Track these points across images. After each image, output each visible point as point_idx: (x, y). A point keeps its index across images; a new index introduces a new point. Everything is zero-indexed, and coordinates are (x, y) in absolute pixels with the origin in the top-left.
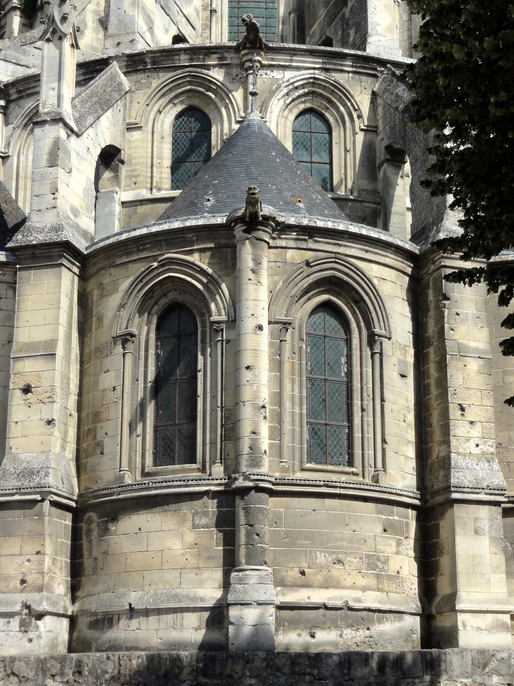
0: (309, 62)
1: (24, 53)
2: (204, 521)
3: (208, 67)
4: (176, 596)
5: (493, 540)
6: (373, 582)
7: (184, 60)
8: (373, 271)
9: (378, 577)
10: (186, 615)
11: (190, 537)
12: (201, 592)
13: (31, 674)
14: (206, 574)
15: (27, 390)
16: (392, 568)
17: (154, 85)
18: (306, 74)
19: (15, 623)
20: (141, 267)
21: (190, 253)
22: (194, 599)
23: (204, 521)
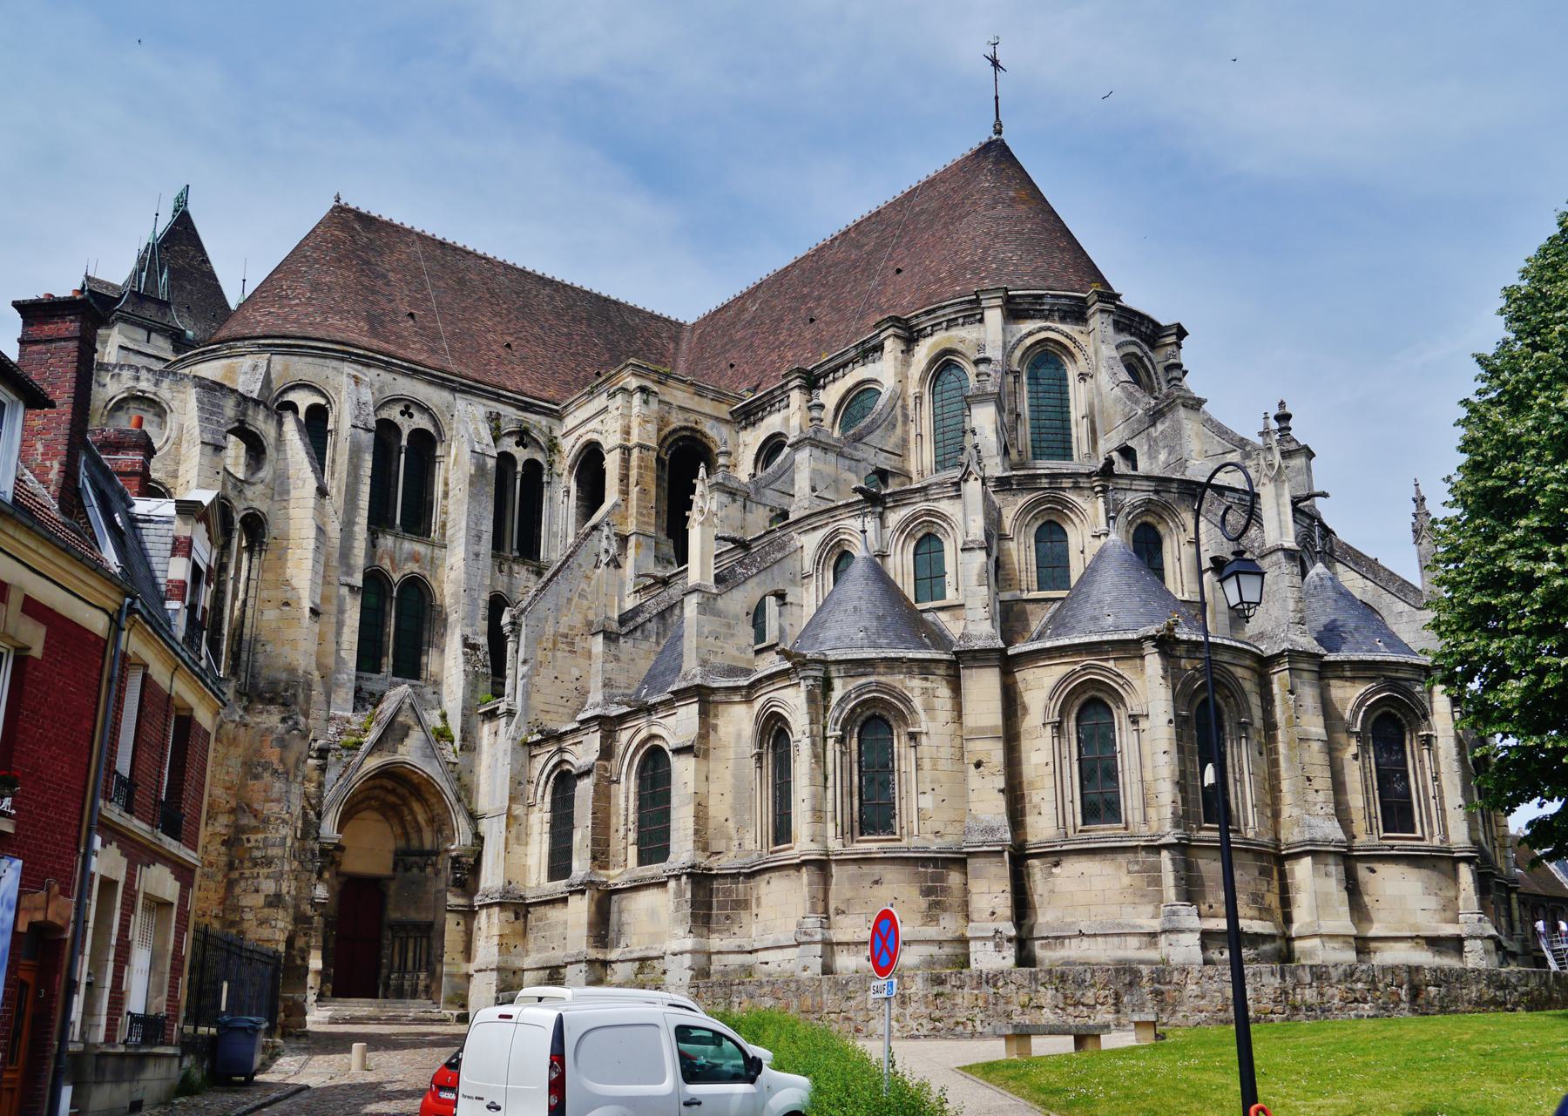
0: (1145, 485)
1: (856, 449)
2: (1136, 868)
3: (1064, 489)
4: (1119, 925)
5: (1339, 881)
6: (1256, 913)
7: (1044, 483)
8: (1239, 672)
9: (1260, 910)
10: (1129, 939)
11: (1126, 880)
12: (1139, 921)
13: (1026, 983)
14: (1141, 908)
15: (978, 765)
16: (1267, 901)
17: (1020, 503)
18: (1143, 496)
19: (990, 945)
20: (1069, 668)
21: (1107, 660)
22: (1134, 927)
23: (1136, 868)
